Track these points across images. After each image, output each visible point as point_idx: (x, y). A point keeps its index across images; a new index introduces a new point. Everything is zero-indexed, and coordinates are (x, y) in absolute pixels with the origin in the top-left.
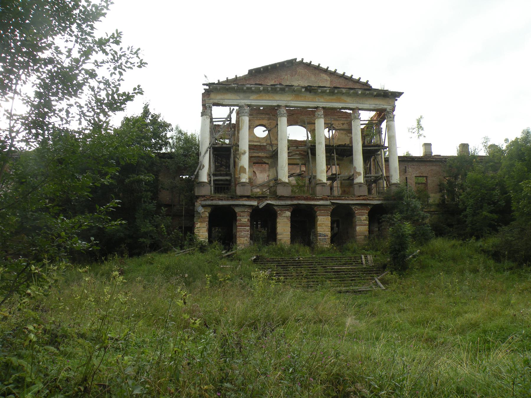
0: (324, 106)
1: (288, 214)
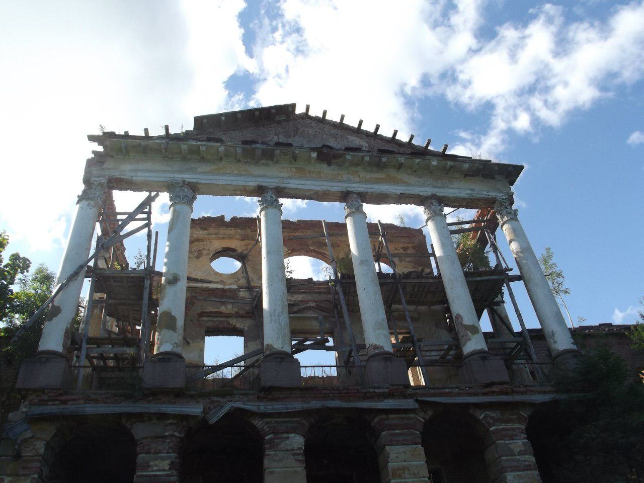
1: (297, 441)
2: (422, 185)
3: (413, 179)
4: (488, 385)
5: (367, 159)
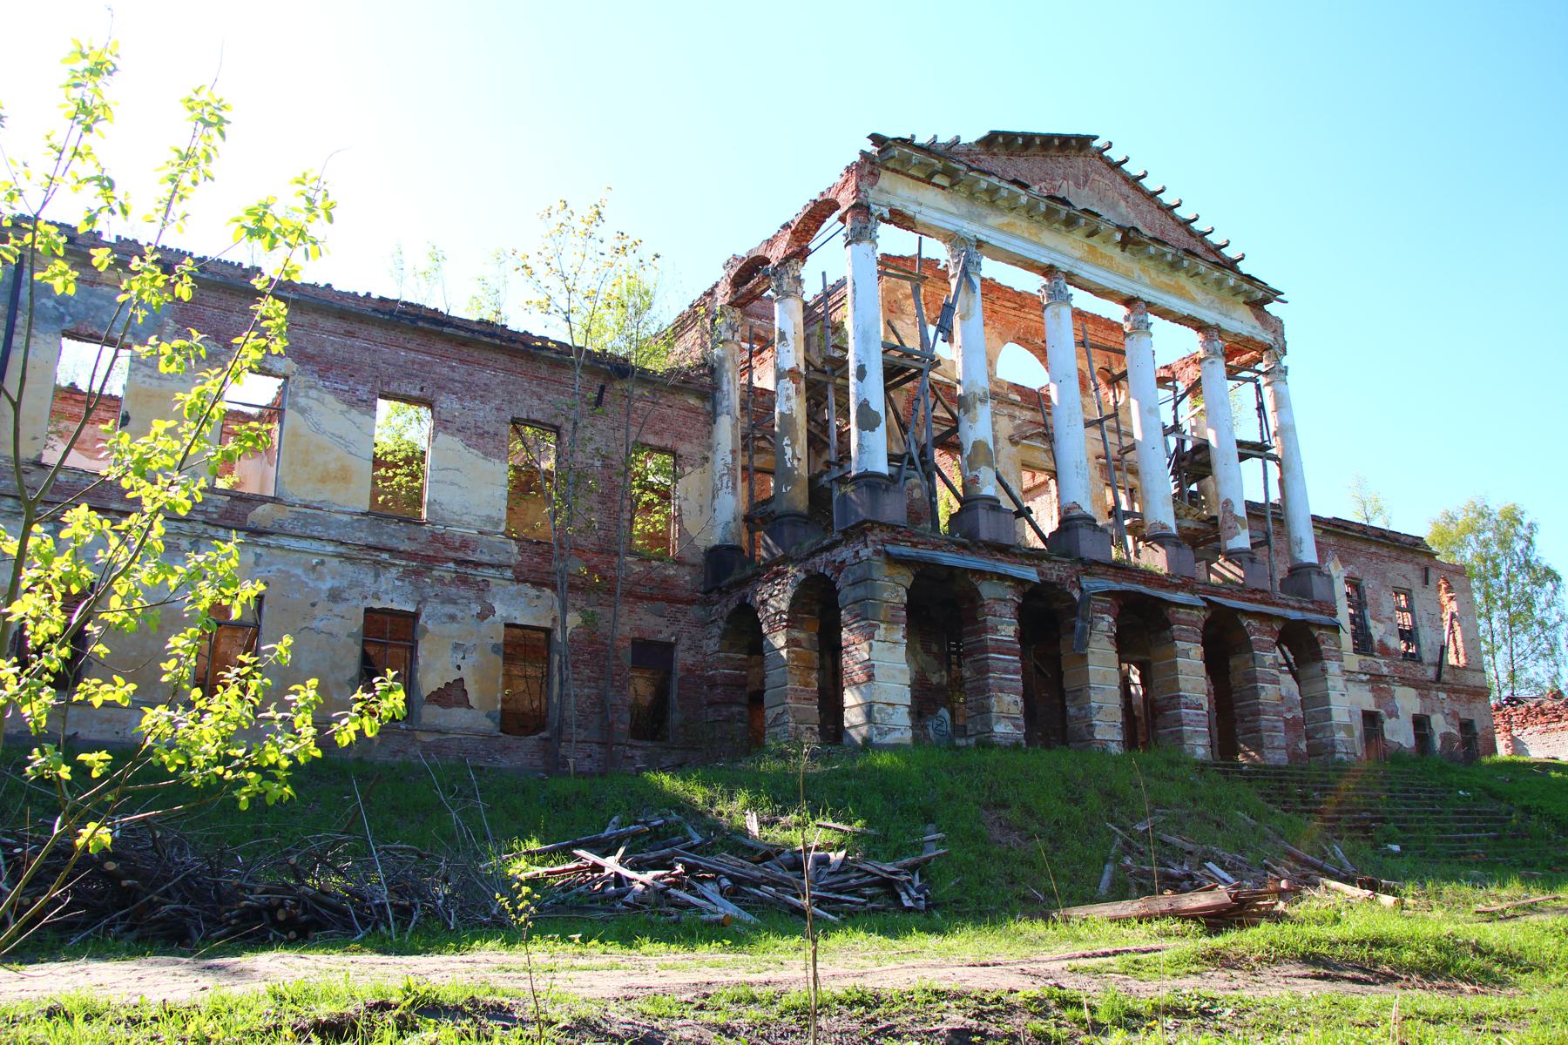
0: (1153, 300)
2: (1208, 308)
3: (1200, 296)
5: (1169, 257)
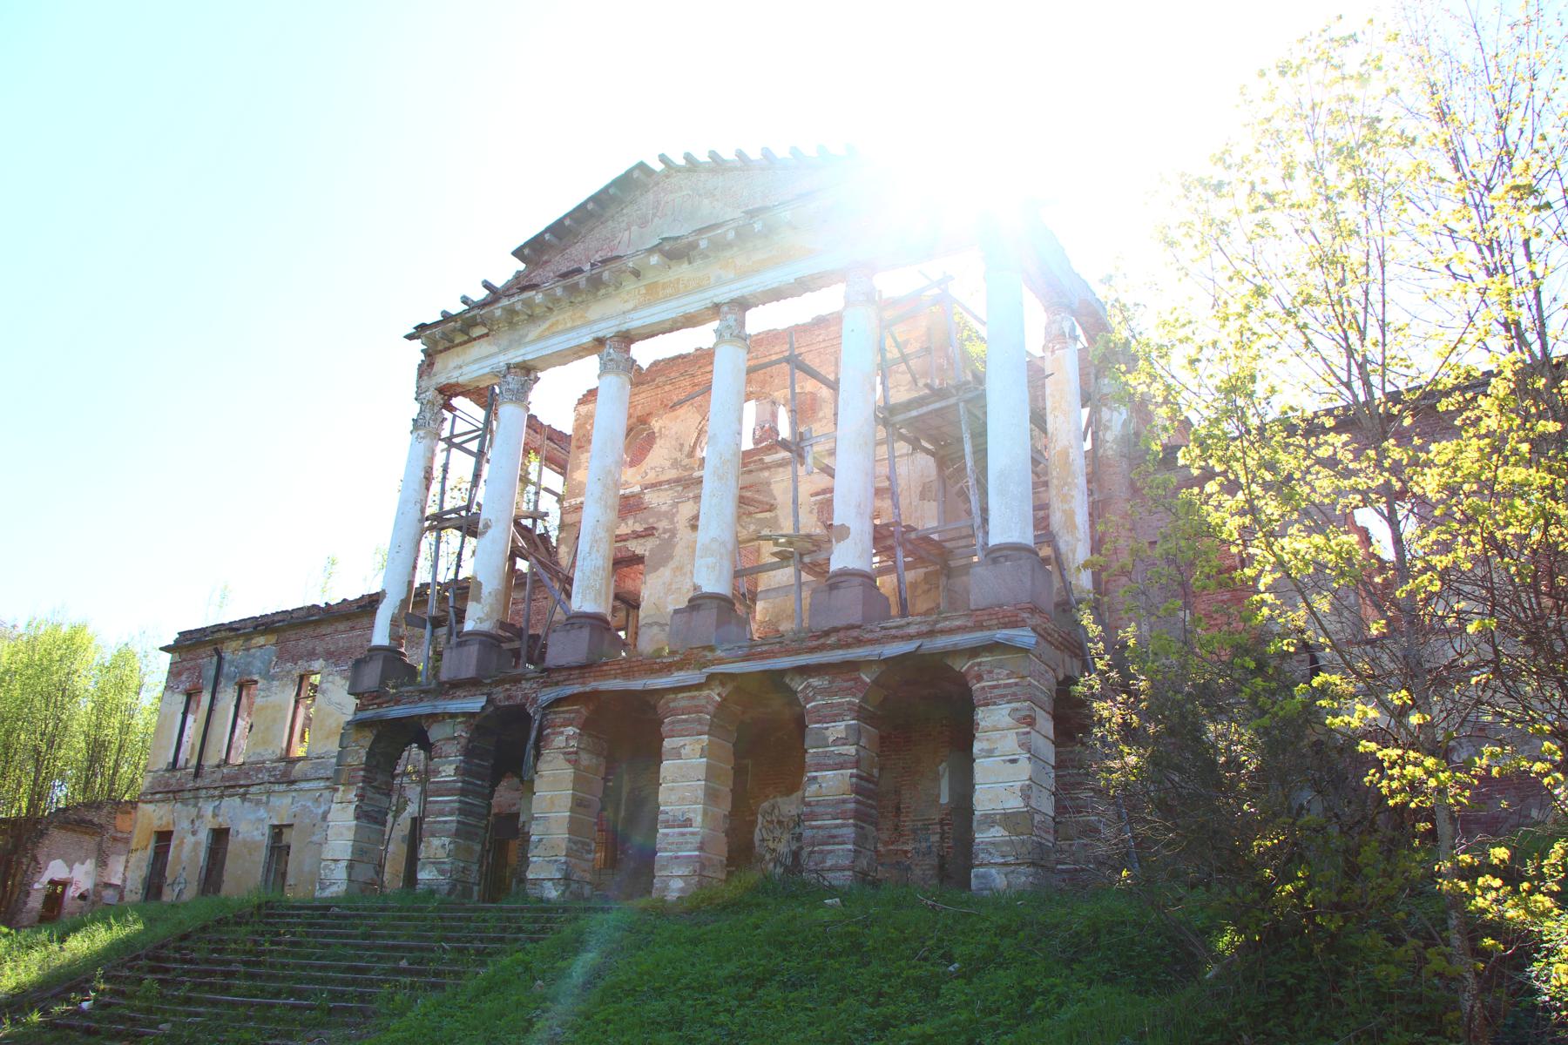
4: (827, 634)
